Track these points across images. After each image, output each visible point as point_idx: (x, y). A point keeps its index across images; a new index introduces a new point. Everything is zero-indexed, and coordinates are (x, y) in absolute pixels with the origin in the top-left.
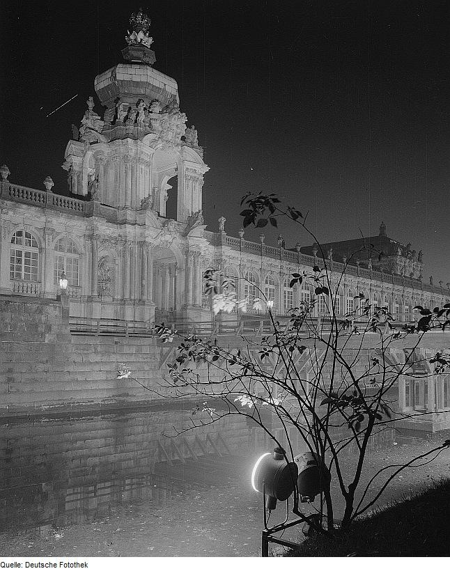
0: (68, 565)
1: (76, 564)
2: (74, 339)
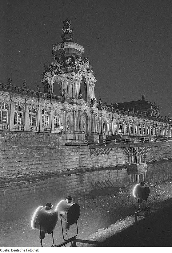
0: (30, 250)
1: (34, 250)
2: (66, 147)
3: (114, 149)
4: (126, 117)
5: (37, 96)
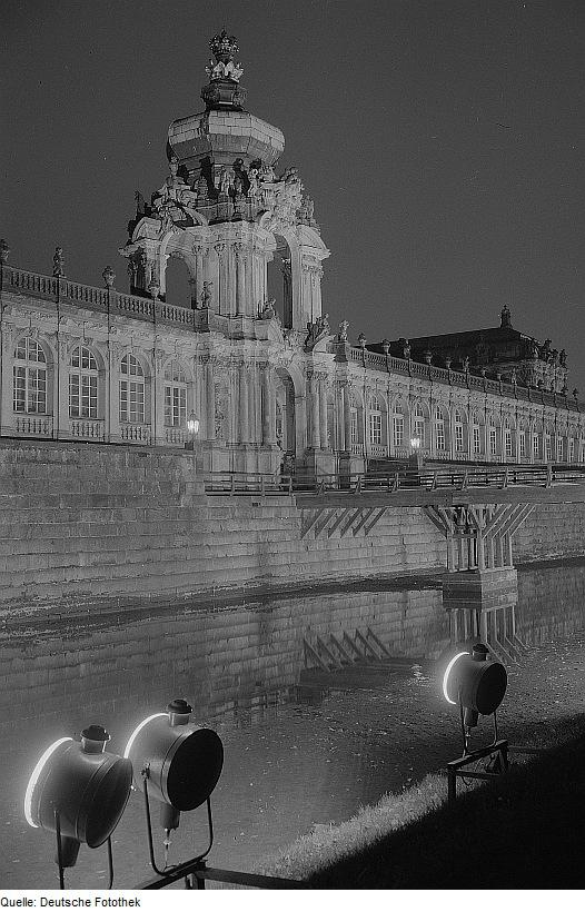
1: (121, 902)
3: (394, 511)
4: (441, 391)
5: (105, 306)
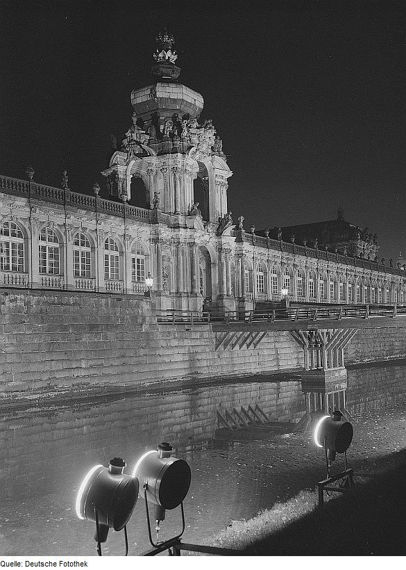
0: (67, 564)
1: (76, 564)
2: (160, 328)
3: (271, 334)
4: (301, 260)
5: (94, 208)
